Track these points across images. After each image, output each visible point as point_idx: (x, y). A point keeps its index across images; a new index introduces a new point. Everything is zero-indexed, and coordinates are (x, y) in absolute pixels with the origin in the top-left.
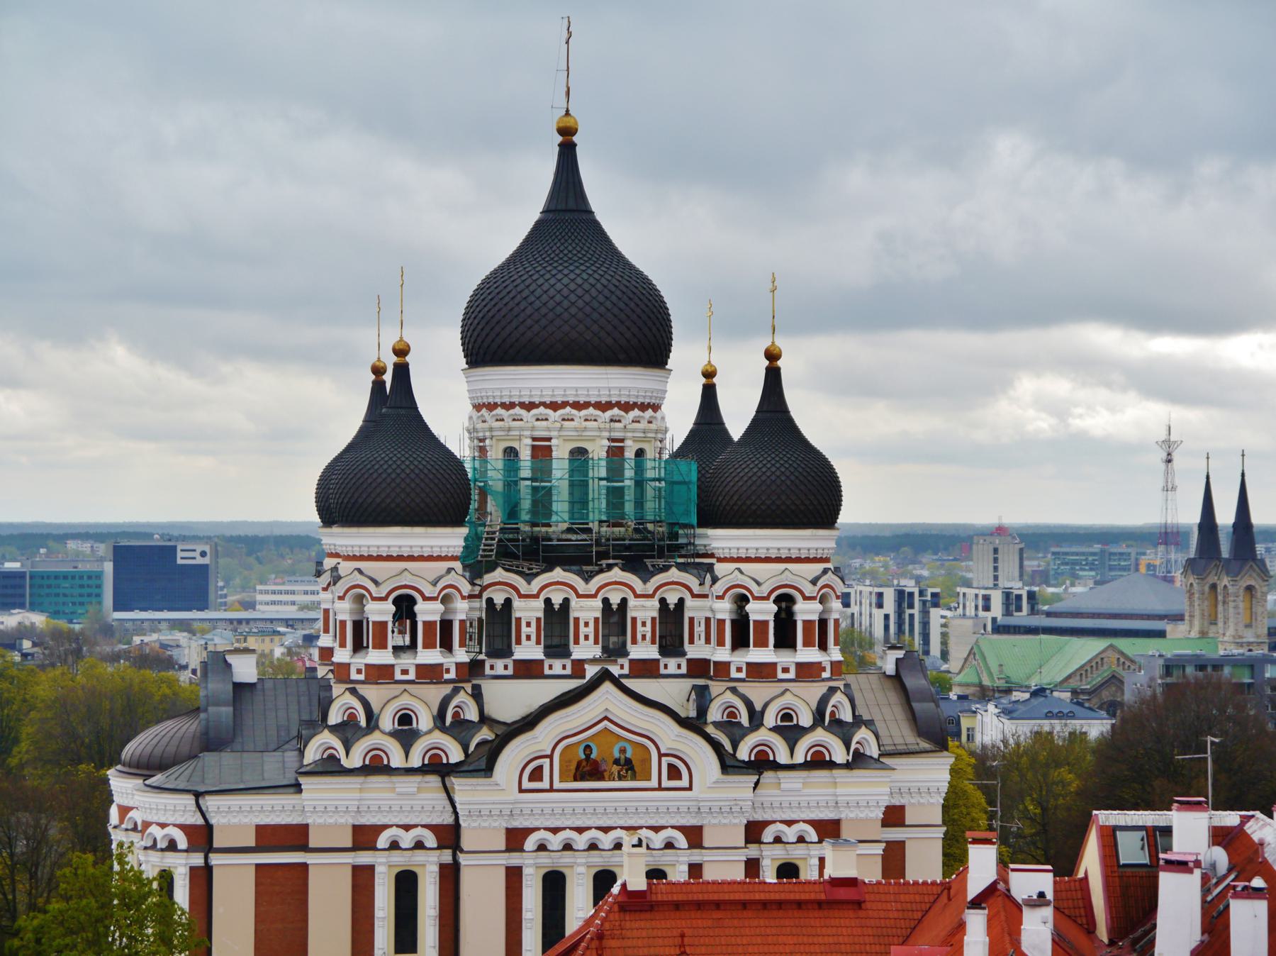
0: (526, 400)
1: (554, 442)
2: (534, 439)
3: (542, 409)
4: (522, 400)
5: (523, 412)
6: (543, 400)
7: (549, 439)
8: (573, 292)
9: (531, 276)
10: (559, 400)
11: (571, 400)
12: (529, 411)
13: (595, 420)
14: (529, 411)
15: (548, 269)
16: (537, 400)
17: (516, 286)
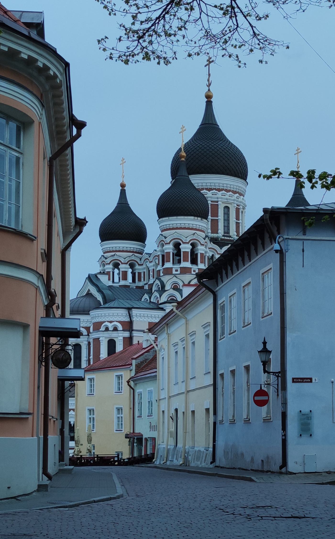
0: (209, 187)
1: (219, 203)
2: (212, 202)
3: (214, 191)
4: (206, 187)
5: (207, 191)
6: (215, 187)
7: (217, 202)
8: (208, 150)
9: (194, 147)
10: (221, 188)
11: (225, 188)
12: (209, 191)
13: (232, 197)
14: (209, 191)
15: (201, 143)
16: (213, 187)
17: (189, 151)
